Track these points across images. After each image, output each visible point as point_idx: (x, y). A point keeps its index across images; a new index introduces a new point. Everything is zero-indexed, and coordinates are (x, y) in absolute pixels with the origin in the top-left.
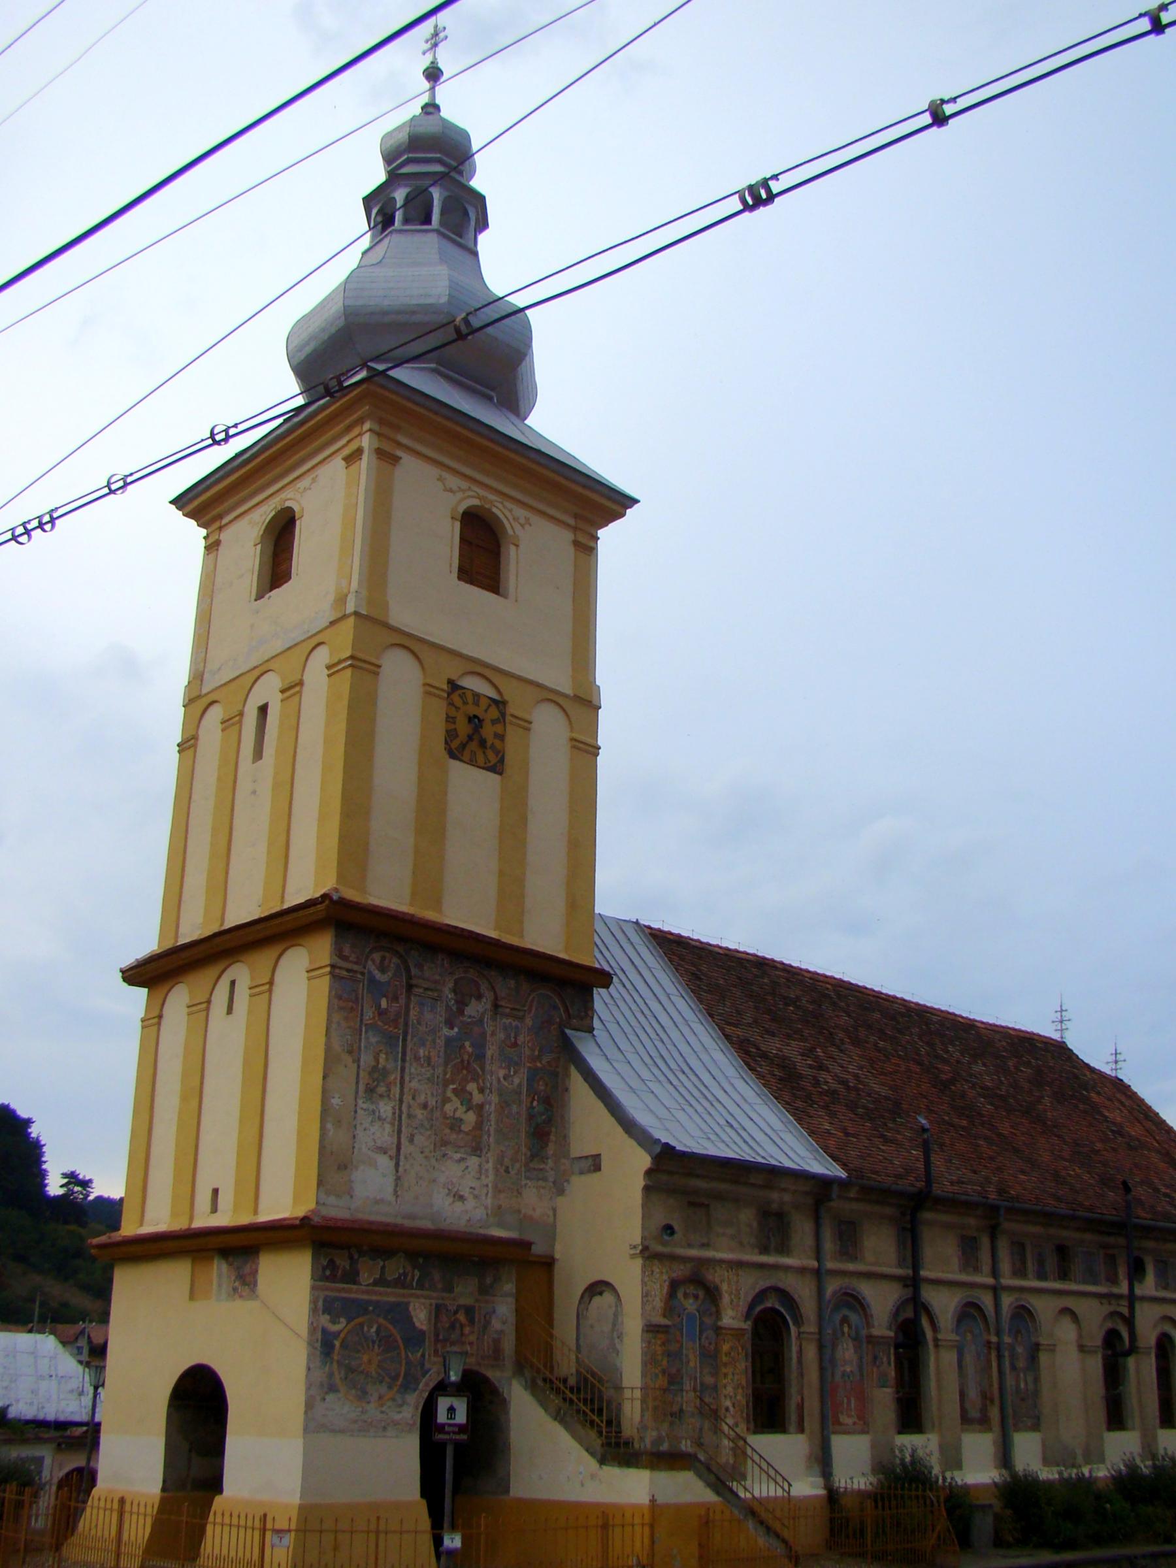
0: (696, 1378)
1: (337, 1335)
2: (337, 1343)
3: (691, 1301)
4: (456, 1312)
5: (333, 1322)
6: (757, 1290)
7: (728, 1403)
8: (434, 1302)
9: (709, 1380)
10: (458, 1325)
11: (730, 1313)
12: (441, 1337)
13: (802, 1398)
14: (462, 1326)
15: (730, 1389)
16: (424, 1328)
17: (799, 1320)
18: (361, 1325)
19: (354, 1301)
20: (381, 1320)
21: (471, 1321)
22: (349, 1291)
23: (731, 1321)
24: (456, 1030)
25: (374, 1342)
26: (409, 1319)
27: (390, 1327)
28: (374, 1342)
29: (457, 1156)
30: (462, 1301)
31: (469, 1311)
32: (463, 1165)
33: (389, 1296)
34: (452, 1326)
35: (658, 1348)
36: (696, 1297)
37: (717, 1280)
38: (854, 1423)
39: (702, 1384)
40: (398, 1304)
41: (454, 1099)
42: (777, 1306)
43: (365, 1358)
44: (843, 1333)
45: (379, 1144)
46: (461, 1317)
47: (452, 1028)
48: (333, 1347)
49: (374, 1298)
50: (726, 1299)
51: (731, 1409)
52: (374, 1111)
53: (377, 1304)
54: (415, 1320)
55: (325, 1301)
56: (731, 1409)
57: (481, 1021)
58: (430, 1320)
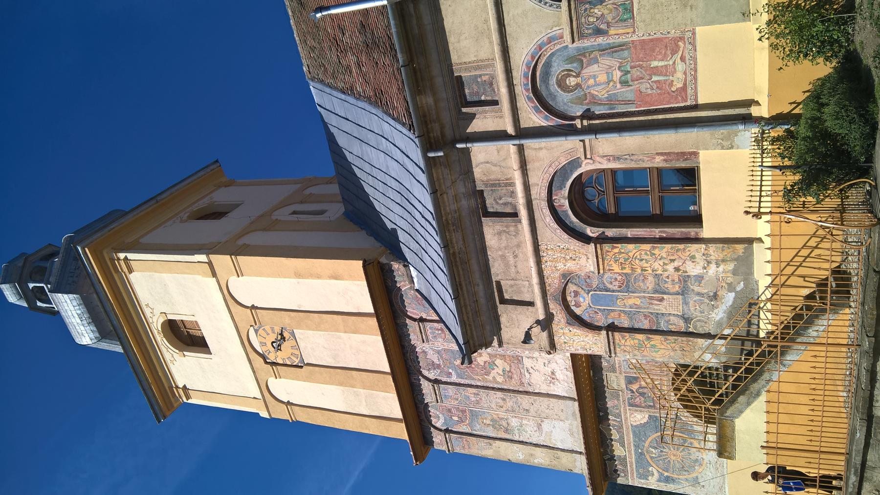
0: (651, 298)
1: (661, 475)
2: (666, 474)
3: (581, 300)
4: (632, 392)
5: (653, 475)
6: (556, 226)
7: (670, 268)
8: (628, 408)
9: (650, 283)
10: (641, 390)
11: (583, 261)
12: (652, 404)
13: (658, 154)
14: (641, 387)
15: (656, 265)
16: (647, 416)
17: (575, 163)
18: (652, 458)
19: (637, 462)
20: (646, 445)
21: (636, 379)
22: (631, 463)
23: (590, 261)
24: (450, 371)
25: (662, 451)
26: (643, 425)
27: (650, 439)
28: (662, 451)
29: (527, 374)
30: (624, 386)
31: (630, 381)
32: (531, 371)
33: (629, 438)
34: (642, 394)
35: (628, 343)
36: (576, 294)
37: (557, 275)
38: (683, 59)
39: (656, 291)
40: (634, 432)
41: (492, 375)
42: (566, 192)
43: (673, 458)
44: (578, 85)
45: (535, 428)
46: (635, 387)
47: (450, 373)
48: (668, 477)
49: (633, 448)
50: (571, 266)
51: (676, 264)
52: (519, 430)
53: (637, 447)
54: (642, 422)
55: (640, 478)
56: (676, 264)
57: (438, 352)
58: (641, 411)
